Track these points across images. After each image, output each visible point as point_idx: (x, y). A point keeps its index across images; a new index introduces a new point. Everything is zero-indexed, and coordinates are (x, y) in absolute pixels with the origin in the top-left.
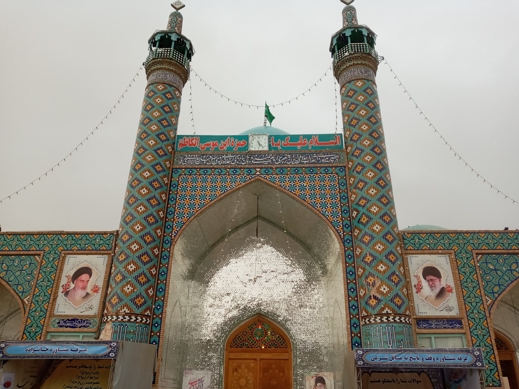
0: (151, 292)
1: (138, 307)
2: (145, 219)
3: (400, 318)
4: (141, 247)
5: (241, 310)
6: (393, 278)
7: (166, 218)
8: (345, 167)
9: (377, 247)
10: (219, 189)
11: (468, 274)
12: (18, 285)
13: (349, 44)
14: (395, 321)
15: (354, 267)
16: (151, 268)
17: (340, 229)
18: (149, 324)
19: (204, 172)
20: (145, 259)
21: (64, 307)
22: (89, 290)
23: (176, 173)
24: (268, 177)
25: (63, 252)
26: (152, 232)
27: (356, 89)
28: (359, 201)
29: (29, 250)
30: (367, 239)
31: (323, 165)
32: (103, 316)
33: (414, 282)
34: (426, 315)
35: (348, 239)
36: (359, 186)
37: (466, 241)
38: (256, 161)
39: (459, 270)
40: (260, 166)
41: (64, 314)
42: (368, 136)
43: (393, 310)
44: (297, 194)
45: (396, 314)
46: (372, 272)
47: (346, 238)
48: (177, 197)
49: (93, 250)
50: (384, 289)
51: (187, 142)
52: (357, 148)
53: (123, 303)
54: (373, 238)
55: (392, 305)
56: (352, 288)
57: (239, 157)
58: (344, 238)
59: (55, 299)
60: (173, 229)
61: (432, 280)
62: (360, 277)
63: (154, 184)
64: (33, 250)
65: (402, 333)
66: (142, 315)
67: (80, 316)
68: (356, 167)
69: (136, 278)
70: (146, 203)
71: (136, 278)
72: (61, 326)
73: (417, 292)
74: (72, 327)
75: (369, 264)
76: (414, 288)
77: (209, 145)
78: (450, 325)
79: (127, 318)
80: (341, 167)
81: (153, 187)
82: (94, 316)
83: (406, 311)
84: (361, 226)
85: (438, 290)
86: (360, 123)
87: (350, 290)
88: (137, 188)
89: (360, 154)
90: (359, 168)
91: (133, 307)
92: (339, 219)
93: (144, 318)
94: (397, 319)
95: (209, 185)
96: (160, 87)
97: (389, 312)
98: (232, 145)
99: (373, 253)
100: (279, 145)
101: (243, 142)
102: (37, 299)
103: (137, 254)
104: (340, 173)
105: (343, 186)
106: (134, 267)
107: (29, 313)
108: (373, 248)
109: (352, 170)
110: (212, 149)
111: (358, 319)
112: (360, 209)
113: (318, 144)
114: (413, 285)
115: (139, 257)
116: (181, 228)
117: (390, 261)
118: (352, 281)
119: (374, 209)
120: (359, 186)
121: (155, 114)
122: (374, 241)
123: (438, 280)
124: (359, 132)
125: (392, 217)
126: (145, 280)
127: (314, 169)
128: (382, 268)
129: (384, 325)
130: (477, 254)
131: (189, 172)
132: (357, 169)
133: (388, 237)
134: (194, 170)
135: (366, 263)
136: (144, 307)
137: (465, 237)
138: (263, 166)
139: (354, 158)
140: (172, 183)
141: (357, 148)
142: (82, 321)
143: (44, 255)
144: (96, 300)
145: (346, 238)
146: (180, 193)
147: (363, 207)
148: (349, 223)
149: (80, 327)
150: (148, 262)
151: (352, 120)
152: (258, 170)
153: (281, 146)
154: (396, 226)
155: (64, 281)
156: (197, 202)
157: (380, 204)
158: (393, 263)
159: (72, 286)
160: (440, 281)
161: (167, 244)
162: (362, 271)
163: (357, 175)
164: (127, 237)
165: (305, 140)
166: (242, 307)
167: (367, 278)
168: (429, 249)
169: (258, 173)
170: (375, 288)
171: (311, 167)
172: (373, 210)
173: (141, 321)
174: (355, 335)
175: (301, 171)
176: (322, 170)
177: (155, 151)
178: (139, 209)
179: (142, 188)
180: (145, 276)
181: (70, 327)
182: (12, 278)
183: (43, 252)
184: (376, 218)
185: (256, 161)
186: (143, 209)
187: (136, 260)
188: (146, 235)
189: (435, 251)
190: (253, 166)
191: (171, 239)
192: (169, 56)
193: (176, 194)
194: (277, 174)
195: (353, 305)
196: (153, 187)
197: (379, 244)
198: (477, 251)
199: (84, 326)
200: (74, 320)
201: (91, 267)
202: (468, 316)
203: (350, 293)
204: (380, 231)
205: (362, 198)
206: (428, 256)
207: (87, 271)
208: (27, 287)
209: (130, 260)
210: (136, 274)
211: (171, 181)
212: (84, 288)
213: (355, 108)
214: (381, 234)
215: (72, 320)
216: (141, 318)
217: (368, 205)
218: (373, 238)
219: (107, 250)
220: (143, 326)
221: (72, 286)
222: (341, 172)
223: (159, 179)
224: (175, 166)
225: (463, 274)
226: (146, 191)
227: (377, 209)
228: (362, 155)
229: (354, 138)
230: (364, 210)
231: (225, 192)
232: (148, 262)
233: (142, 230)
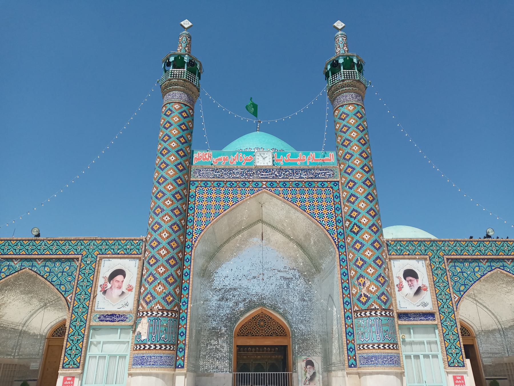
0: (178, 291)
1: (169, 304)
2: (171, 227)
3: (386, 312)
4: (168, 252)
5: (247, 303)
6: (380, 279)
7: (187, 225)
8: (338, 182)
9: (367, 253)
10: (231, 199)
11: (440, 276)
12: (60, 285)
13: (342, 70)
14: (382, 315)
15: (347, 269)
16: (177, 270)
17: (335, 236)
18: (177, 318)
19: (217, 184)
20: (172, 262)
21: (103, 304)
22: (124, 289)
23: (193, 185)
24: (273, 190)
25: (99, 256)
26: (177, 239)
27: (348, 112)
28: (351, 213)
29: (68, 254)
31: (320, 180)
32: (138, 311)
33: (396, 282)
34: (406, 309)
35: (342, 245)
36: (351, 199)
37: (438, 248)
38: (262, 175)
39: (432, 272)
40: (266, 180)
41: (103, 310)
42: (358, 156)
43: (380, 306)
44: (299, 205)
46: (363, 274)
47: (340, 244)
48: (195, 207)
49: (125, 254)
50: (373, 288)
51: (201, 156)
52: (349, 166)
53: (156, 300)
54: (363, 245)
55: (379, 302)
56: (346, 287)
57: (248, 171)
58: (338, 245)
59: (94, 297)
60: (193, 235)
61: (411, 280)
62: (352, 278)
63: (176, 196)
64: (72, 254)
65: (386, 325)
66: (172, 311)
67: (117, 312)
68: (348, 183)
69: (166, 279)
70: (171, 214)
71: (166, 279)
72: (102, 321)
73: (399, 291)
74: (111, 321)
75: (360, 268)
76: (396, 287)
77: (221, 159)
78: (425, 318)
79: (160, 313)
80: (335, 181)
81: (176, 198)
82: (130, 312)
83: (390, 306)
84: (353, 235)
85: (416, 289)
86: (351, 144)
87: (344, 288)
88: (162, 200)
89: (352, 172)
90: (351, 184)
91: (164, 303)
92: (334, 227)
93: (173, 313)
94: (383, 313)
95: (222, 196)
96: (177, 106)
97: (377, 308)
98: (241, 160)
99: (363, 257)
100: (281, 160)
101: (250, 157)
102: (79, 297)
103: (166, 258)
104: (334, 187)
105: (337, 198)
106: (163, 270)
107: (73, 310)
108: (363, 254)
109: (345, 185)
110: (224, 163)
111: (351, 313)
113: (315, 160)
114: (395, 285)
115: (167, 261)
116: (200, 234)
117: (378, 265)
118: (346, 281)
119: (364, 221)
120: (351, 199)
121: (173, 132)
122: (364, 248)
123: (415, 280)
124: (351, 152)
125: (379, 227)
126: (173, 280)
127: (312, 183)
128: (370, 271)
129: (372, 318)
130: (447, 259)
131: (204, 184)
132: (349, 185)
133: (375, 245)
134: (208, 183)
135: (358, 266)
136: (173, 304)
137: (437, 245)
138: (269, 180)
139: (347, 175)
140: (191, 194)
141: (349, 166)
143: (82, 259)
144: (131, 298)
145: (340, 244)
146: (197, 203)
147: (355, 218)
148: (342, 231)
149: (118, 321)
150: (175, 265)
151: (344, 141)
152: (264, 183)
153: (283, 162)
154: (382, 235)
155: (101, 281)
157: (369, 216)
158: (380, 267)
159: (109, 285)
160: (417, 281)
161: (188, 248)
162: (354, 273)
163: (349, 190)
164: (156, 243)
165: (304, 157)
166: (247, 300)
167: (358, 279)
168: (409, 255)
169: (264, 186)
170: (365, 288)
171: (310, 182)
172: (363, 221)
173: (171, 316)
174: (348, 326)
175: (301, 185)
176: (319, 184)
177: (176, 166)
178: (165, 218)
179: (167, 199)
180: (173, 277)
181: (109, 321)
182: (54, 279)
183: (81, 256)
184: (366, 228)
185: (262, 175)
186: (168, 218)
187: (165, 263)
188: (172, 241)
189: (413, 257)
190: (260, 180)
191: (192, 244)
192: (183, 77)
193: (194, 204)
194: (281, 187)
195: (347, 301)
196: (176, 198)
197: (368, 251)
198: (447, 257)
199: (122, 320)
200: (112, 315)
201: (124, 269)
202: (439, 310)
203: (344, 291)
204: (369, 239)
205: (354, 210)
206: (407, 261)
207: (121, 272)
208: (68, 287)
209: (159, 263)
210: (165, 275)
211: (189, 192)
212: (120, 287)
213: (347, 130)
214: (370, 242)
215: (111, 315)
216: (172, 313)
217: (359, 217)
218: (363, 245)
219: (137, 254)
220: (173, 320)
221: (109, 285)
222: (335, 186)
223: (180, 191)
224: (192, 179)
225: (436, 275)
226: (170, 203)
227: (366, 221)
228: (354, 172)
229: (346, 157)
230: (356, 221)
231: (236, 203)
232: (175, 265)
233: (168, 237)
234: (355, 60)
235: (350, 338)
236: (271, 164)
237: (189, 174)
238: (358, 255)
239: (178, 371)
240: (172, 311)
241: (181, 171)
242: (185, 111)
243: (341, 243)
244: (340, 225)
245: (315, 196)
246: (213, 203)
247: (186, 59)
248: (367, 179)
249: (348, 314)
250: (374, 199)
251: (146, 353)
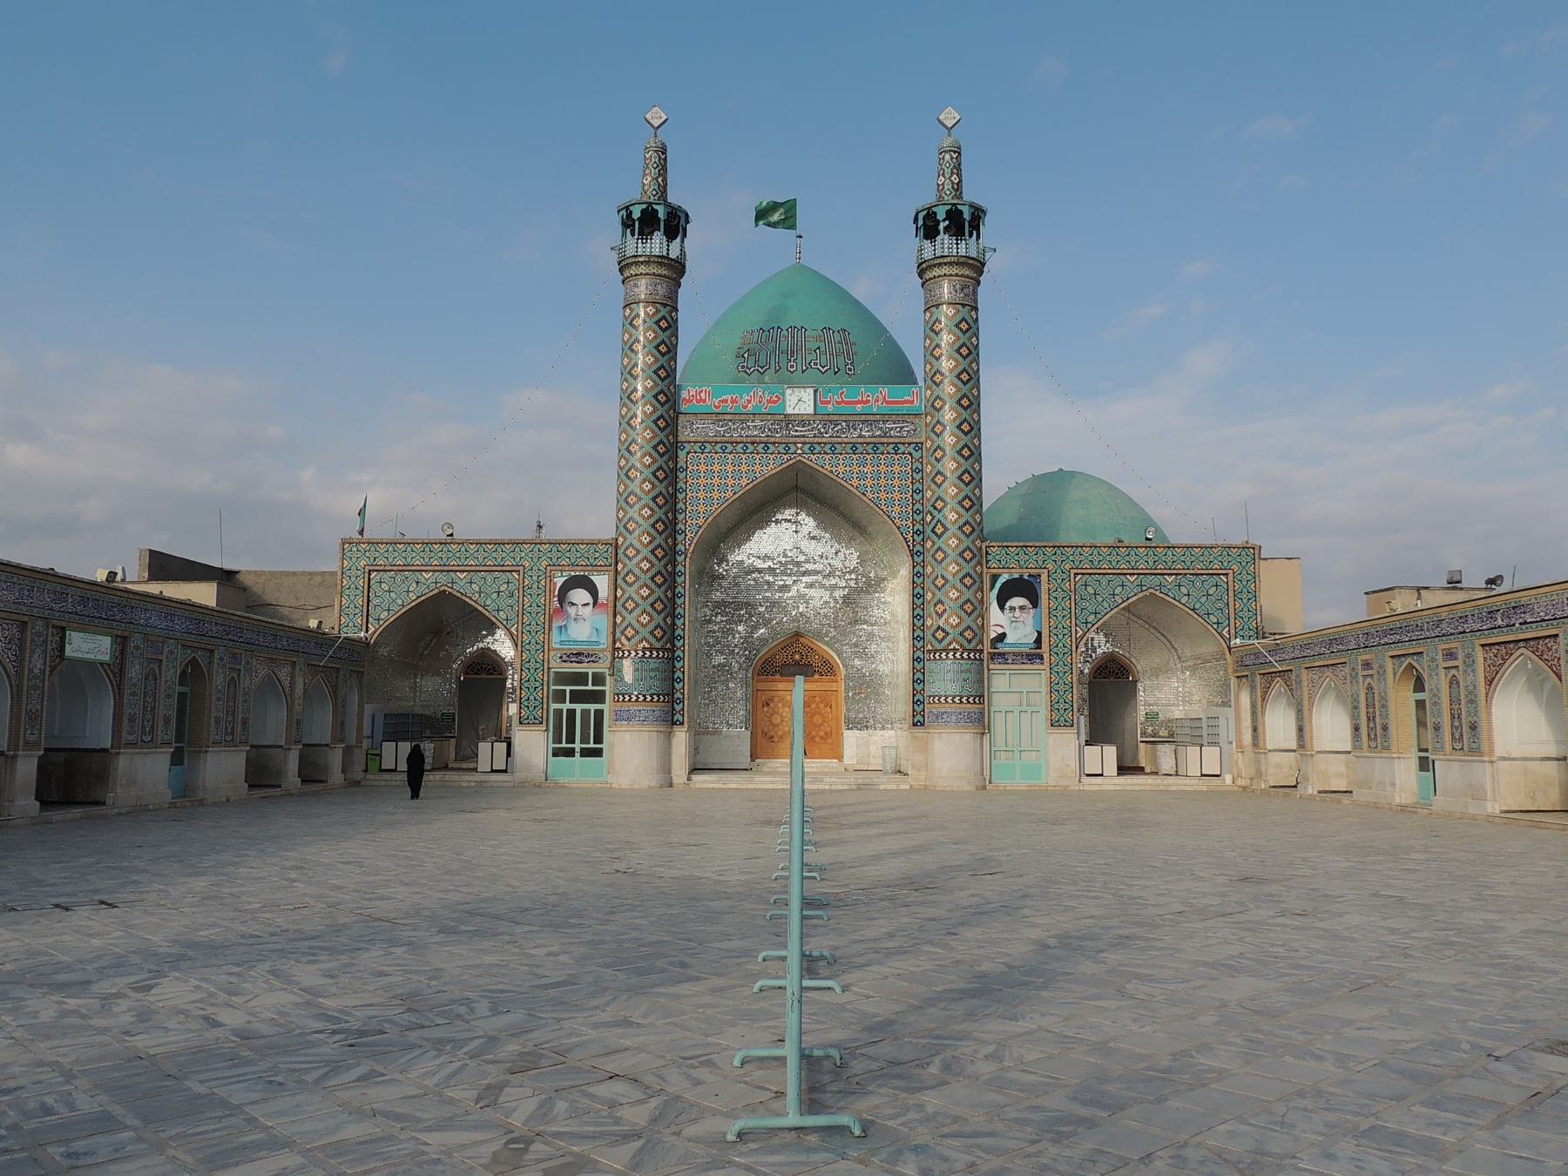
0: (669, 620)
1: (658, 640)
30: (940, 556)
32: (615, 649)
66: (663, 649)
103: (650, 574)
112: (935, 513)
142: (588, 655)
156: (716, 495)
175: (860, 449)
176: (890, 448)
200: (579, 654)
208: (512, 615)
210: (651, 600)
234: (967, 216)
235: (919, 688)
236: (811, 411)
237: (675, 433)
238: (939, 570)
239: (676, 728)
240: (663, 649)
241: (662, 430)
242: (664, 318)
243: (918, 548)
244: (918, 518)
245: (883, 468)
246: (716, 481)
247: (662, 212)
248: (966, 445)
249: (919, 654)
250: (973, 479)
251: (633, 708)
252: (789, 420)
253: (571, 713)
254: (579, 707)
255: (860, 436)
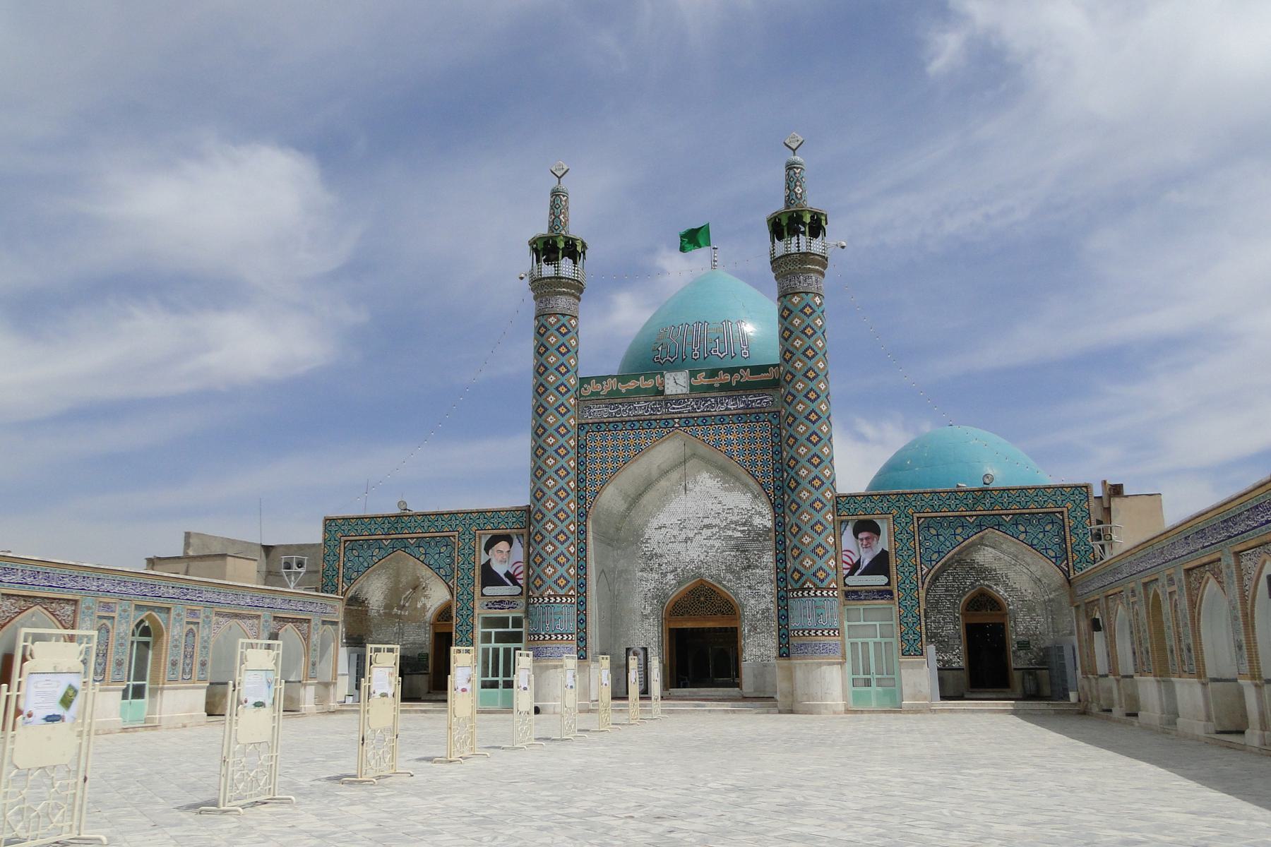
45: (817, 588)
79: (553, 600)
176: (752, 418)
252: (669, 401)
253: (496, 651)
254: (501, 646)
255: (727, 409)
